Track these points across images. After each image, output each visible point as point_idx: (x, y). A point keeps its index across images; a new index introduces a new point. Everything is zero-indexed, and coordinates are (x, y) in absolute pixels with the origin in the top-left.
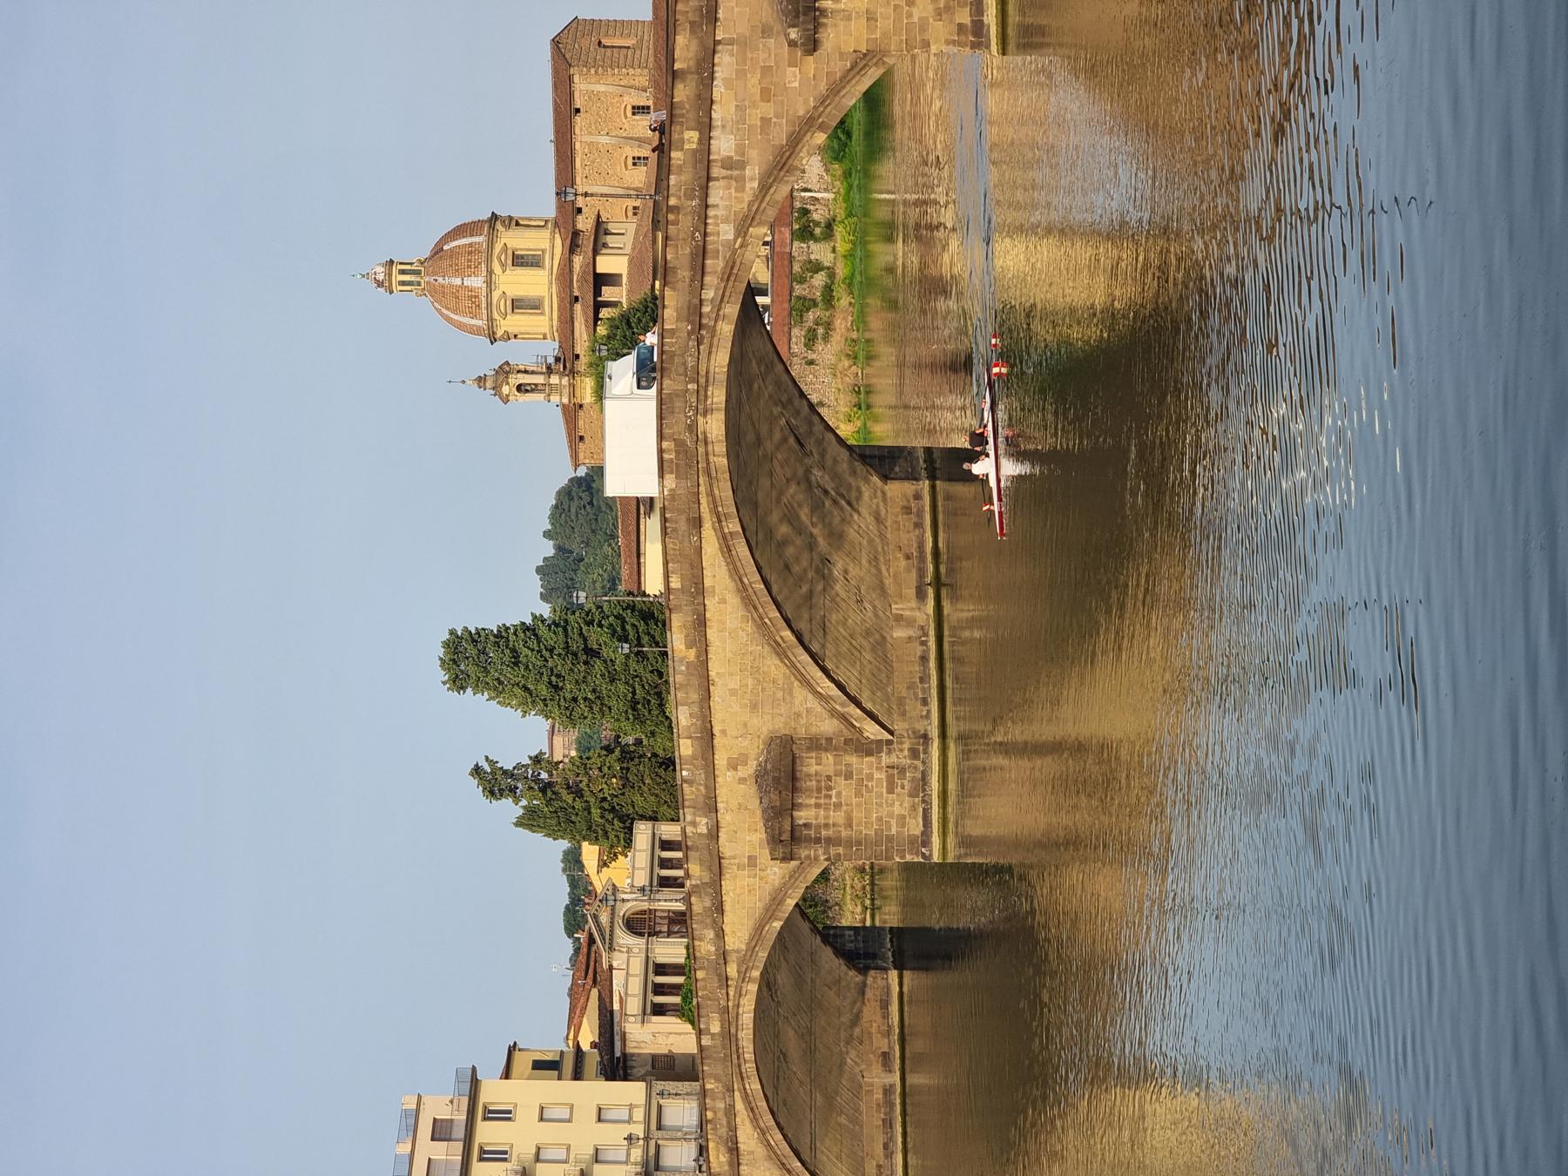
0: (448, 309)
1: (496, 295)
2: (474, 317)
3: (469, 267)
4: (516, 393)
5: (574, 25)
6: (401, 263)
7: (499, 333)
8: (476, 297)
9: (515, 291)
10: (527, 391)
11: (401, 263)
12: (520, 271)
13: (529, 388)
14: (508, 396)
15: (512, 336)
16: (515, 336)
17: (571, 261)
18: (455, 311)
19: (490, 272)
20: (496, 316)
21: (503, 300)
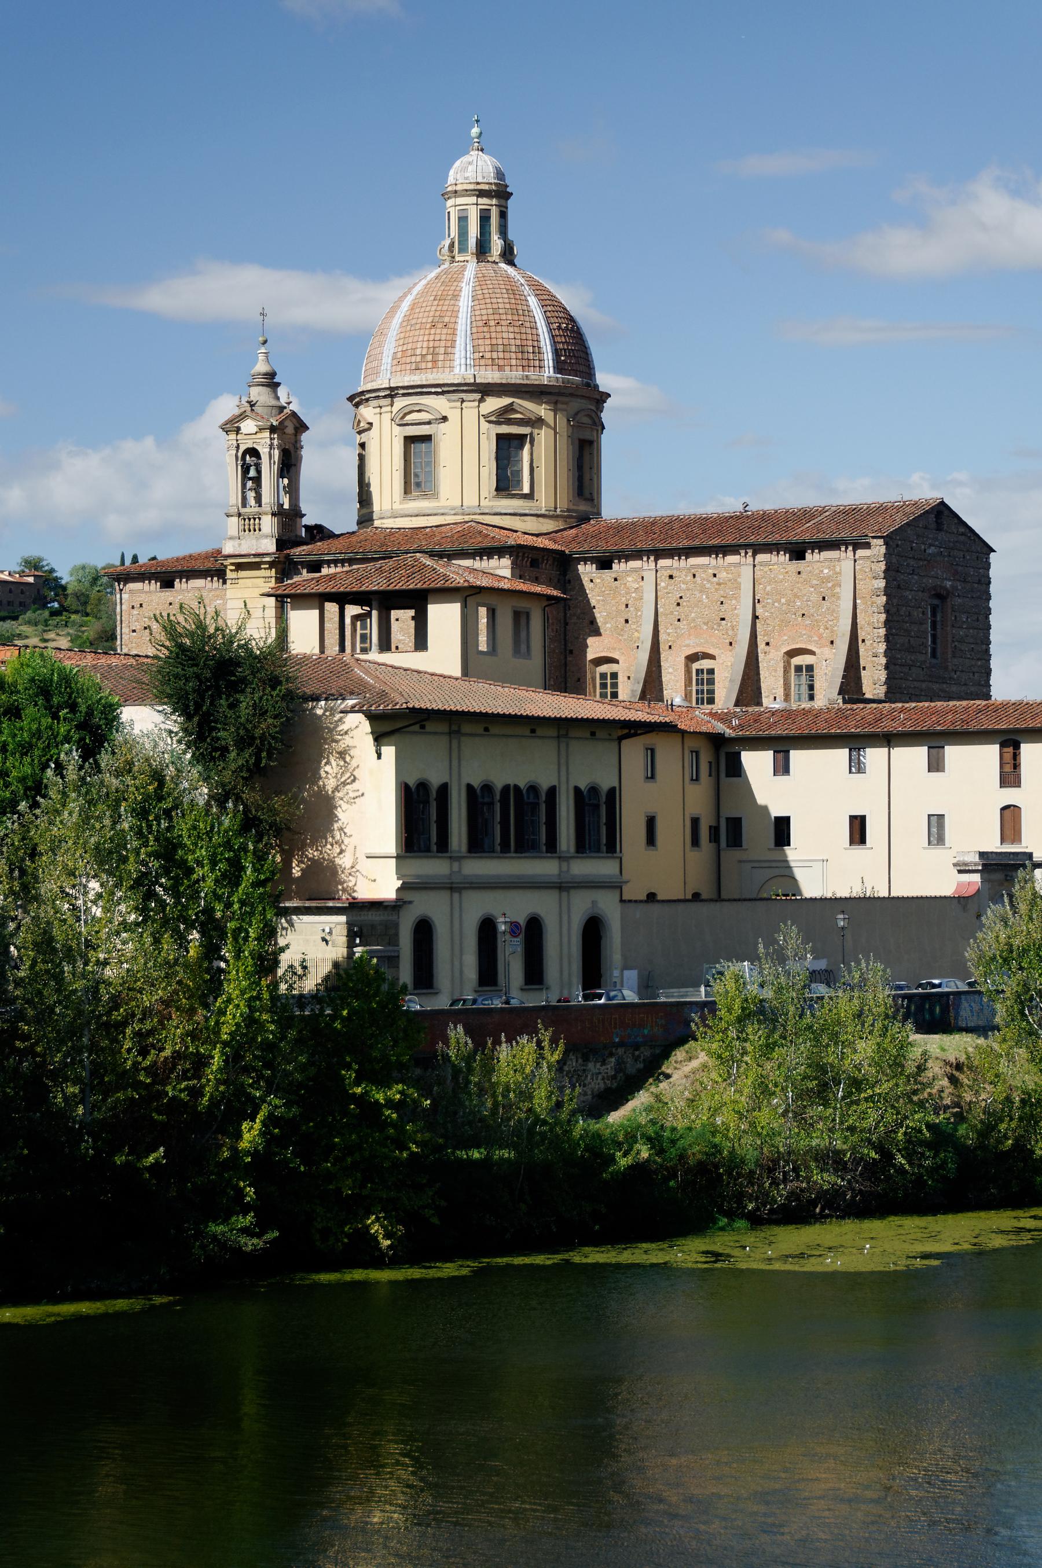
0: (412, 308)
1: (439, 404)
2: (398, 361)
3: (493, 348)
4: (242, 448)
5: (985, 549)
6: (503, 215)
7: (367, 412)
8: (434, 361)
9: (446, 438)
10: (246, 469)
11: (503, 215)
12: (489, 447)
13: (252, 473)
14: (238, 430)
15: (364, 438)
16: (362, 445)
17: (499, 551)
18: (407, 319)
19: (485, 390)
20: (400, 403)
21: (424, 416)
